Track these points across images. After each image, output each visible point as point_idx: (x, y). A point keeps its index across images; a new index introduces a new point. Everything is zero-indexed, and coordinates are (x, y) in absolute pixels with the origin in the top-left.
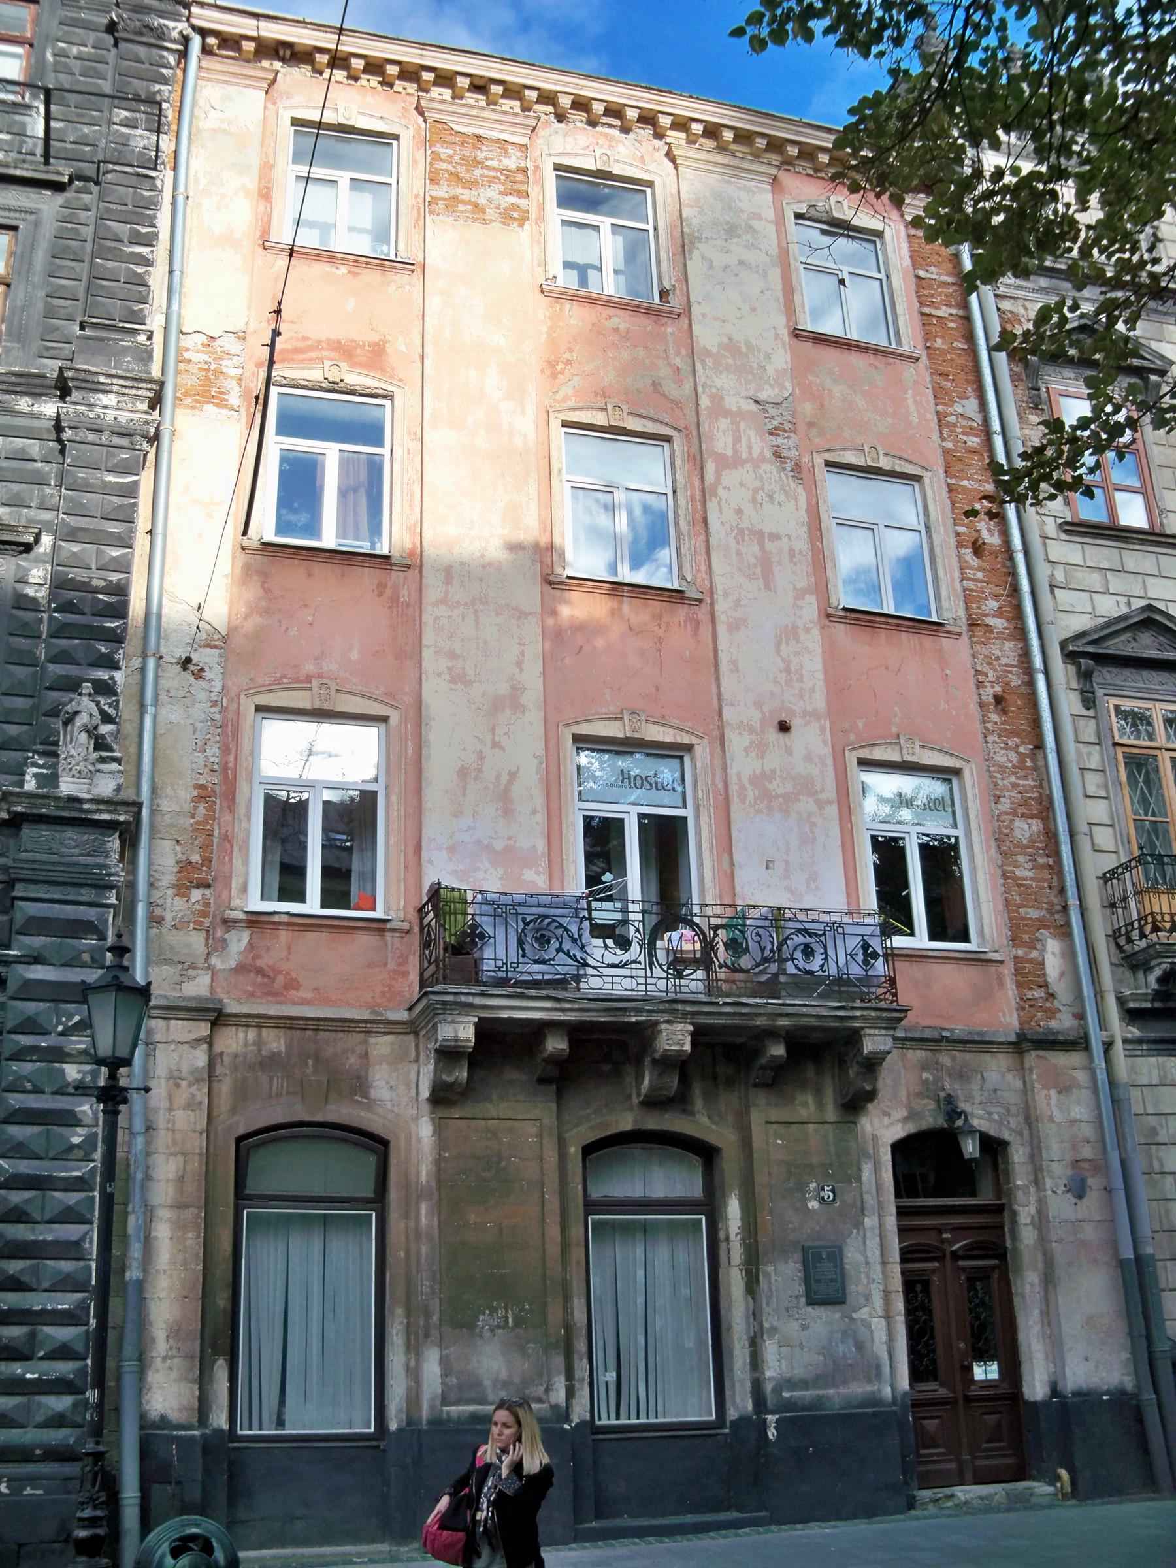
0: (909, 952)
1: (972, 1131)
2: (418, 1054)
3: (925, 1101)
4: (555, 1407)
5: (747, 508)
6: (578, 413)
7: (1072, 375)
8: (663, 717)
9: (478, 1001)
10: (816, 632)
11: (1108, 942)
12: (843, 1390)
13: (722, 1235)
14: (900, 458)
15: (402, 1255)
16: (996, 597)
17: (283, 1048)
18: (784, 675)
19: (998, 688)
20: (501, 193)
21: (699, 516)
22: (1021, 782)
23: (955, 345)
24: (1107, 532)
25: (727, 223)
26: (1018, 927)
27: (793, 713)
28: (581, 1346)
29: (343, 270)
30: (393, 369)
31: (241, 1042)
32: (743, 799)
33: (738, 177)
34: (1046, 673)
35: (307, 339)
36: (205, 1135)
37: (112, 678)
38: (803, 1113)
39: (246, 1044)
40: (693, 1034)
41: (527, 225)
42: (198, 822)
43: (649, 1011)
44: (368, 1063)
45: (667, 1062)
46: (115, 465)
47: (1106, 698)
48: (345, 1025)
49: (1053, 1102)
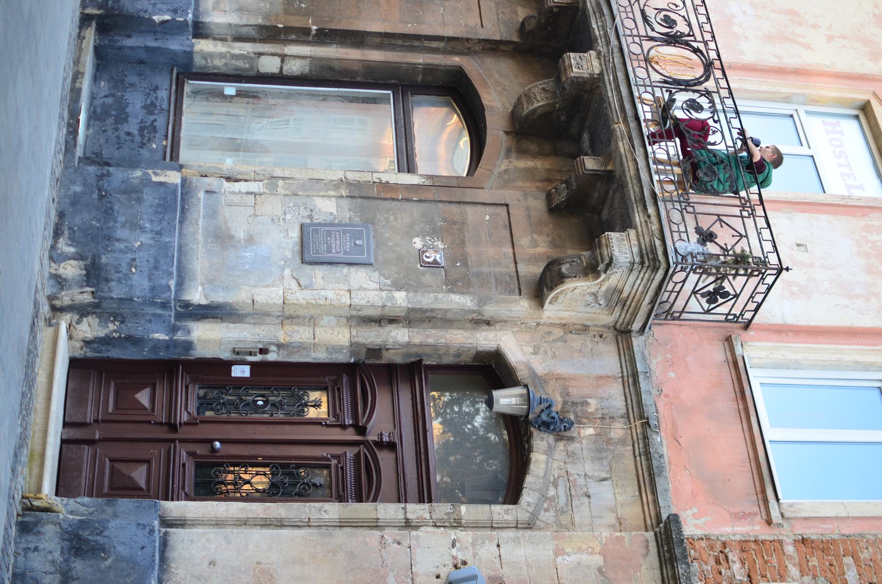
0: (748, 392)
32: (867, 229)
49: (585, 558)
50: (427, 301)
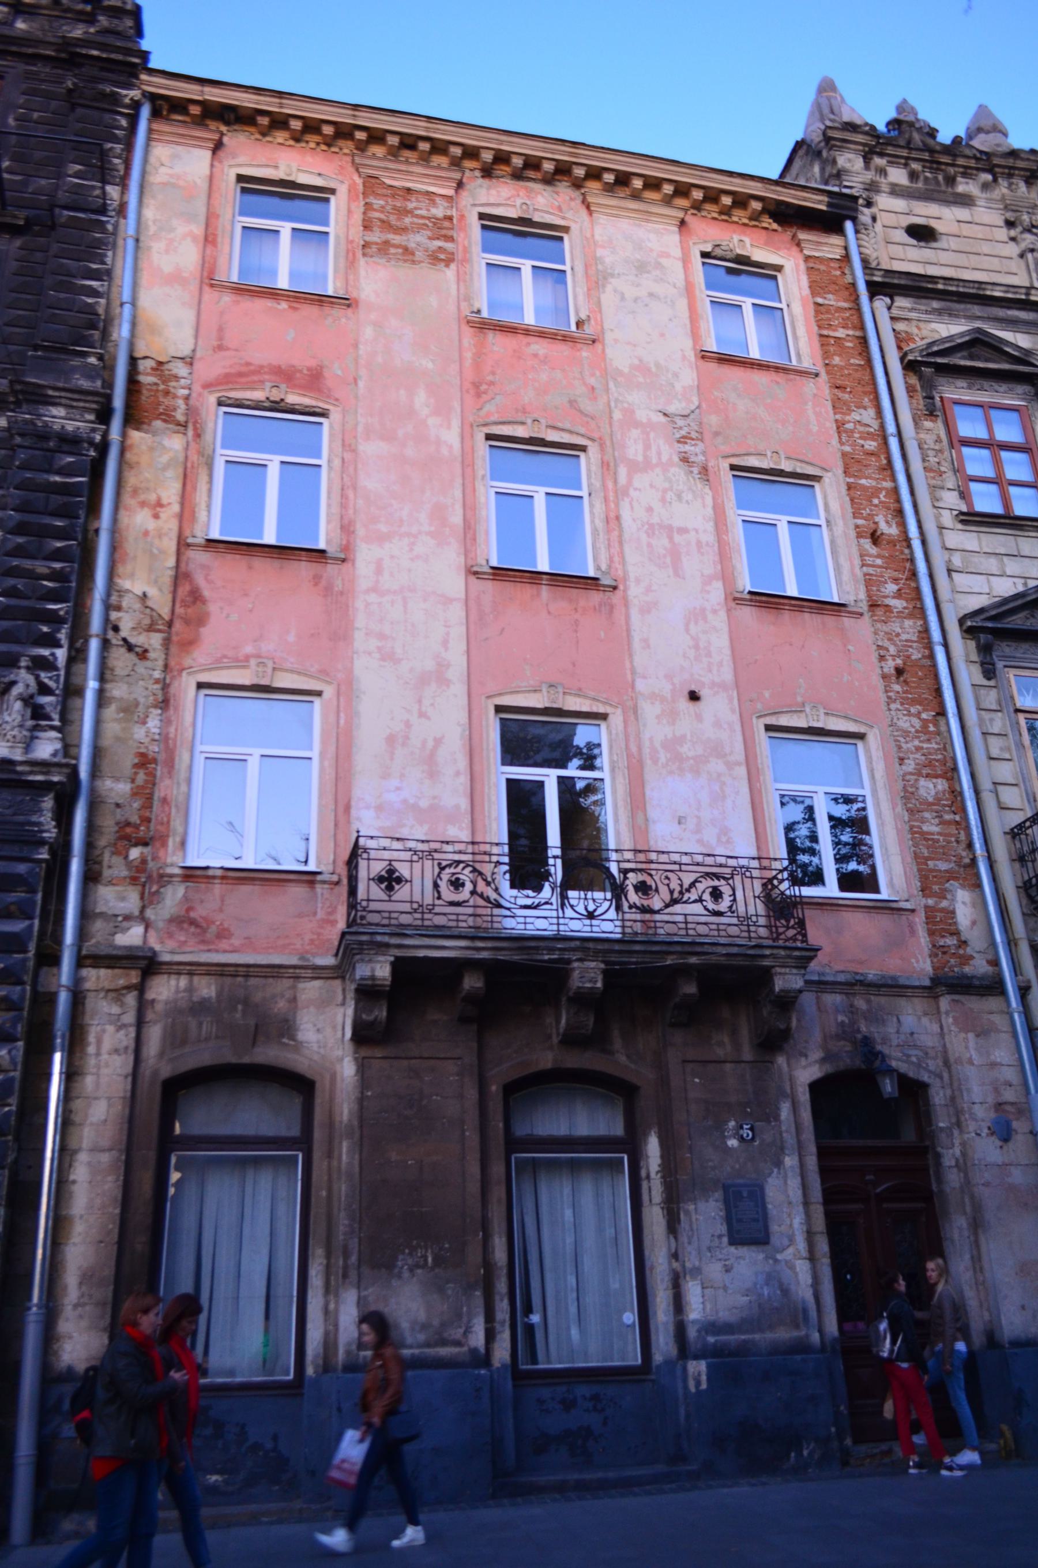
0: (820, 901)
1: (891, 1071)
2: (344, 998)
3: (842, 1043)
4: (474, 1351)
5: (657, 505)
6: (500, 427)
7: (965, 385)
8: (580, 689)
9: (394, 941)
10: (723, 614)
11: (1019, 893)
12: (769, 1335)
13: (643, 1173)
14: (801, 461)
15: (324, 1193)
16: (896, 580)
17: (213, 994)
18: (693, 651)
19: (899, 661)
20: (430, 238)
21: (612, 515)
22: (925, 745)
23: (852, 361)
24: (1002, 521)
25: (638, 261)
26: (926, 877)
27: (703, 684)
28: (501, 1286)
29: (284, 305)
30: (329, 390)
31: (173, 989)
32: (655, 761)
33: (648, 221)
34: (946, 645)
35: (248, 364)
36: (130, 1079)
37: (53, 654)
38: (720, 1052)
39: (177, 991)
40: (605, 972)
41: (453, 266)
42: (138, 787)
43: (560, 949)
44: (296, 1007)
45: (583, 1000)
46: (62, 468)
47: (1006, 669)
48: (275, 971)
50: (790, 1139)
